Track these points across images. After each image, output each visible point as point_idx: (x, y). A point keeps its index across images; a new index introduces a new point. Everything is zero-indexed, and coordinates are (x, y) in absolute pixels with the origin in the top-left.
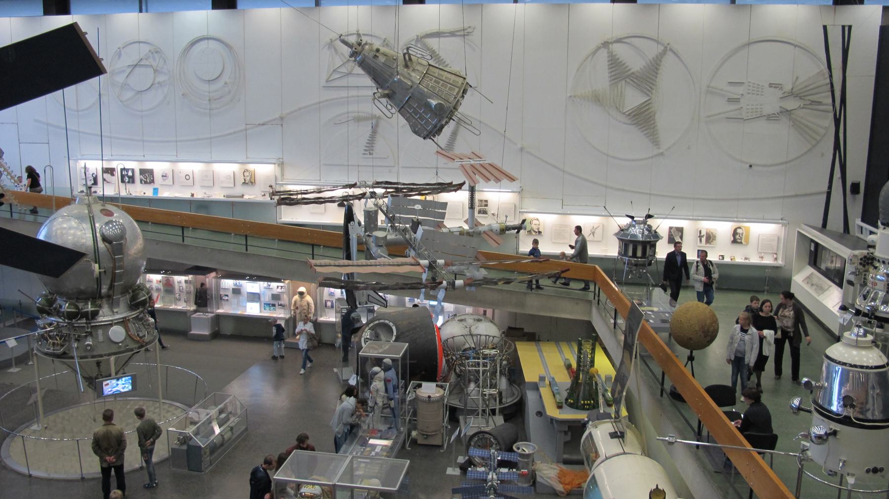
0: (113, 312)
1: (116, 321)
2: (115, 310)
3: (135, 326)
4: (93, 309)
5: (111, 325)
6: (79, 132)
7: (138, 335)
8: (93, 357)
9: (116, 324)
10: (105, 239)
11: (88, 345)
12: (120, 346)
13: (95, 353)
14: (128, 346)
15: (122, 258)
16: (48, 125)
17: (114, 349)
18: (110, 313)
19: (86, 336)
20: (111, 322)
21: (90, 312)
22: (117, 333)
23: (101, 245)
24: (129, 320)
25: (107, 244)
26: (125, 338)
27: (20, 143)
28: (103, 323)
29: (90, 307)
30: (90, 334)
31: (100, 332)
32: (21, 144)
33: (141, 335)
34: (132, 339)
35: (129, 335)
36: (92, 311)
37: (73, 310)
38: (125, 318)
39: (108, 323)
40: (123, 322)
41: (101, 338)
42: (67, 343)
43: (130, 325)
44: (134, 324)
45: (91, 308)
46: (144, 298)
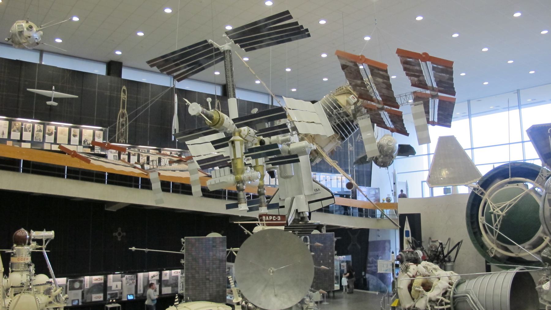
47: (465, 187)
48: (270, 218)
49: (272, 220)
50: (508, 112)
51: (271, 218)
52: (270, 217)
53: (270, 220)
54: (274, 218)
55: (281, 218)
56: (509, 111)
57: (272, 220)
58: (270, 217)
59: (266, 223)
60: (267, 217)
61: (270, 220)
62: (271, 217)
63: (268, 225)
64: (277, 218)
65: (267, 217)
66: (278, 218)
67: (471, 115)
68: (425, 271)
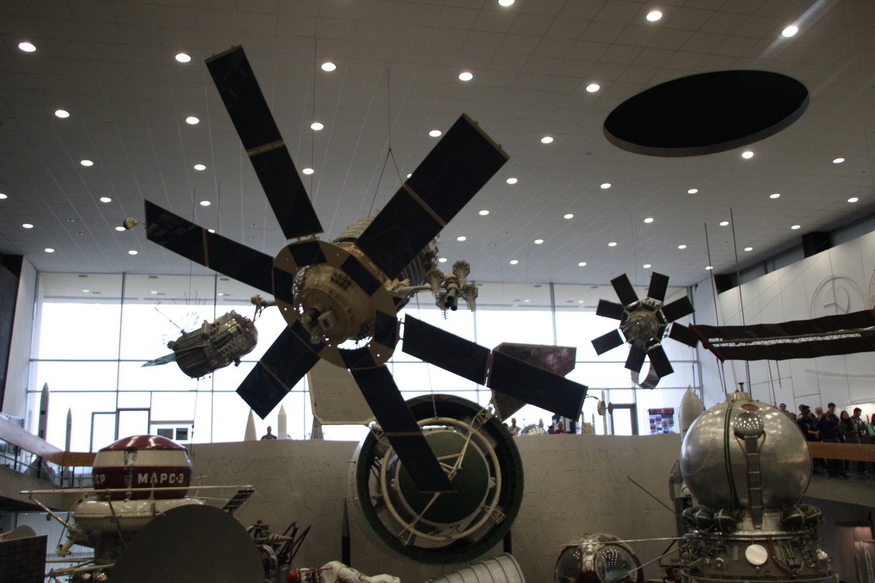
0: (754, 526)
1: (757, 539)
2: (757, 526)
3: (786, 552)
4: (724, 517)
5: (750, 543)
6: (847, 376)
7: (787, 562)
8: (724, 577)
9: (756, 542)
10: (738, 434)
11: (719, 562)
12: (758, 571)
13: (726, 573)
14: (768, 571)
15: (748, 453)
16: (818, 373)
17: (751, 573)
18: (752, 528)
19: (720, 552)
20: (750, 539)
21: (720, 519)
22: (757, 555)
23: (733, 441)
24: (775, 541)
25: (739, 439)
26: (767, 562)
27: (795, 398)
28: (742, 539)
29: (720, 514)
30: (723, 551)
31: (736, 549)
32: (796, 399)
33: (791, 563)
34: (777, 565)
35: (773, 559)
36: (722, 519)
37: (705, 517)
38: (771, 536)
39: (746, 539)
40: (767, 542)
41: (736, 557)
42: (701, 558)
43: (777, 549)
44: (784, 548)
45: (722, 515)
46: (797, 515)
47: (365, 426)
48: (164, 476)
49: (166, 484)
50: (549, 313)
51: (165, 479)
52: (162, 475)
53: (161, 482)
54: (173, 478)
55: (184, 478)
56: (122, 303)
57: (166, 484)
58: (162, 475)
59: (156, 492)
60: (155, 475)
61: (161, 482)
62: (165, 475)
63: (159, 496)
64: (177, 478)
65: (155, 475)
66: (180, 478)
67: (125, 299)
68: (357, 578)
